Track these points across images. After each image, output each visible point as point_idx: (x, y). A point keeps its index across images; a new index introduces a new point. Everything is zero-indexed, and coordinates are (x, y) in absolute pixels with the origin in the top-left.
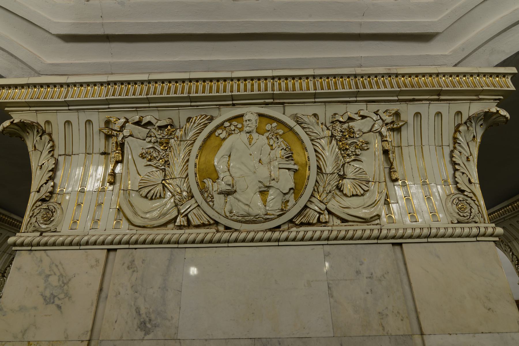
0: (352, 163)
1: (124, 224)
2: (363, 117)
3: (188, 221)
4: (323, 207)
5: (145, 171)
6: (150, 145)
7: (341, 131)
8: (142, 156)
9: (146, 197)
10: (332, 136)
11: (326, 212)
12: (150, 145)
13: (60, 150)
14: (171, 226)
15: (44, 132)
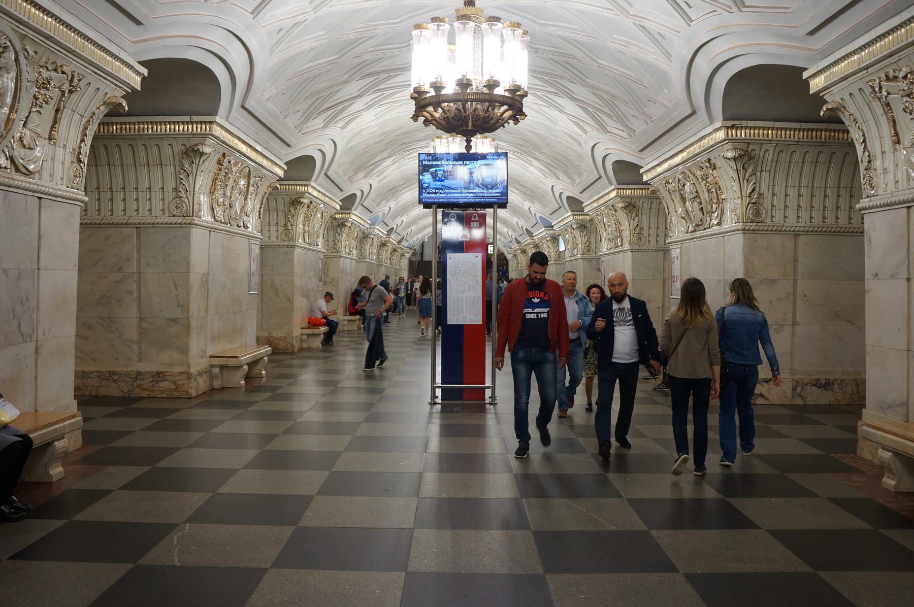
13: (860, 120)
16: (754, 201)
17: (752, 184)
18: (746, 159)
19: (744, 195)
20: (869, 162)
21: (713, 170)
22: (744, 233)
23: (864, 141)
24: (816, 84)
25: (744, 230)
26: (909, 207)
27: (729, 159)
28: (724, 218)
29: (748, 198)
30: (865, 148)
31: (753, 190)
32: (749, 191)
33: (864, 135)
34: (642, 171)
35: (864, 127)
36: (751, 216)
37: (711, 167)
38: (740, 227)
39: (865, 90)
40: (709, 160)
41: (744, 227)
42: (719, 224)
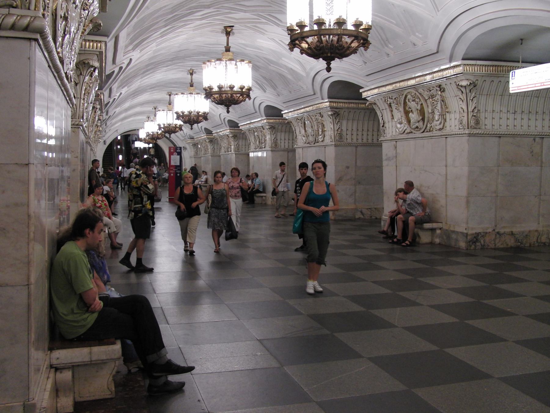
16: (475, 114)
17: (474, 103)
18: (472, 86)
19: (470, 110)
21: (441, 92)
22: (469, 136)
25: (470, 134)
28: (447, 124)
29: (472, 113)
31: (475, 108)
32: (473, 107)
34: (361, 91)
36: (473, 124)
37: (440, 91)
38: (467, 132)
41: (469, 132)
42: (440, 129)
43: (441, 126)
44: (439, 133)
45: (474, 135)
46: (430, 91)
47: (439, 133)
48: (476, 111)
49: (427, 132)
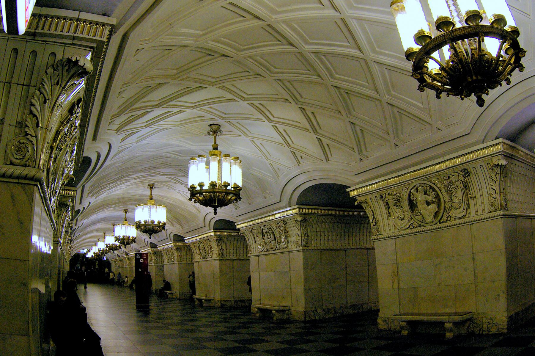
0: (456, 195)
1: (397, 230)
2: (453, 176)
3: (413, 227)
4: (448, 215)
5: (397, 211)
6: (395, 202)
7: (448, 183)
8: (394, 205)
9: (400, 220)
10: (445, 186)
11: (449, 217)
12: (395, 202)
13: (372, 207)
14: (409, 229)
15: (367, 203)
16: (305, 238)
20: (376, 222)
21: (284, 225)
23: (373, 215)
24: (353, 194)
25: (303, 250)
26: (395, 238)
27: (298, 221)
30: (374, 217)
33: (373, 213)
35: (373, 210)
38: (301, 249)
39: (378, 197)
40: (284, 220)
42: (286, 248)
43: (286, 246)
44: (286, 250)
45: (307, 250)
46: (278, 224)
47: (286, 250)
48: (306, 236)
49: (278, 250)
